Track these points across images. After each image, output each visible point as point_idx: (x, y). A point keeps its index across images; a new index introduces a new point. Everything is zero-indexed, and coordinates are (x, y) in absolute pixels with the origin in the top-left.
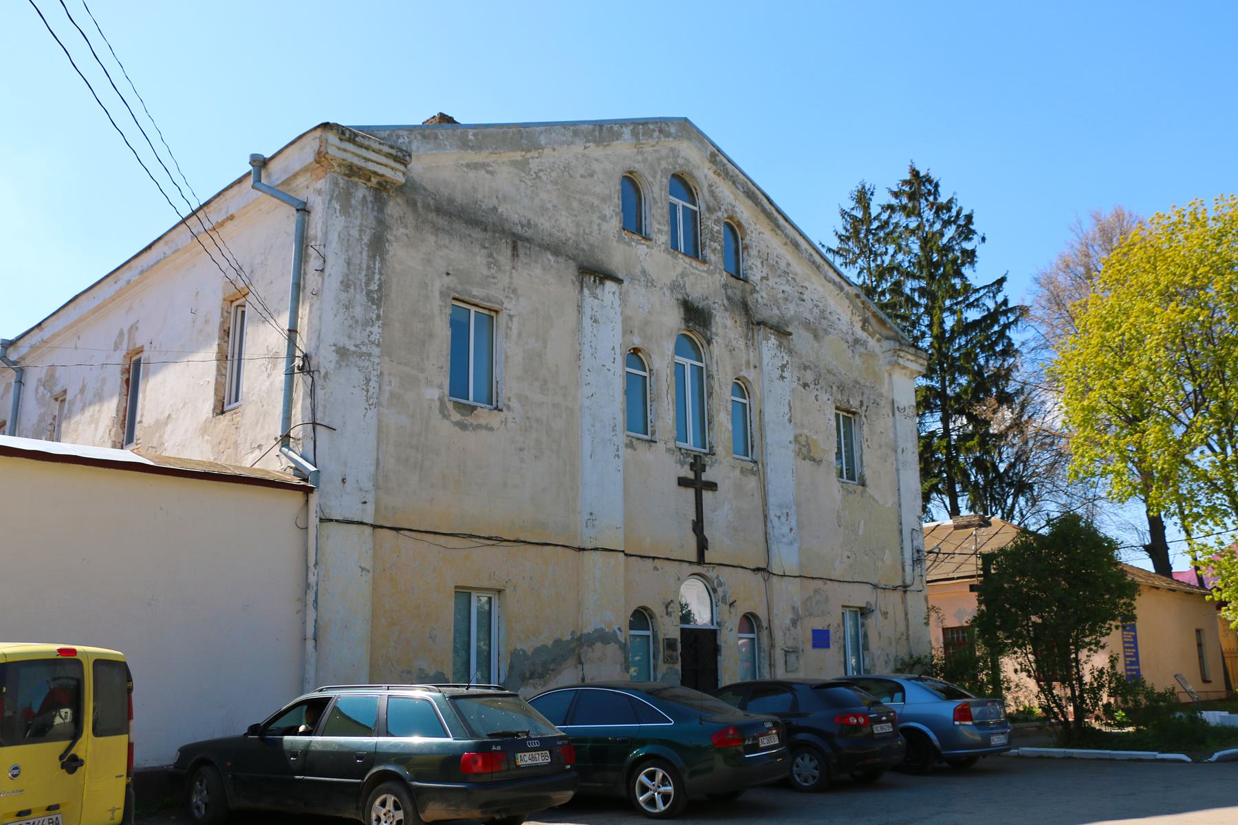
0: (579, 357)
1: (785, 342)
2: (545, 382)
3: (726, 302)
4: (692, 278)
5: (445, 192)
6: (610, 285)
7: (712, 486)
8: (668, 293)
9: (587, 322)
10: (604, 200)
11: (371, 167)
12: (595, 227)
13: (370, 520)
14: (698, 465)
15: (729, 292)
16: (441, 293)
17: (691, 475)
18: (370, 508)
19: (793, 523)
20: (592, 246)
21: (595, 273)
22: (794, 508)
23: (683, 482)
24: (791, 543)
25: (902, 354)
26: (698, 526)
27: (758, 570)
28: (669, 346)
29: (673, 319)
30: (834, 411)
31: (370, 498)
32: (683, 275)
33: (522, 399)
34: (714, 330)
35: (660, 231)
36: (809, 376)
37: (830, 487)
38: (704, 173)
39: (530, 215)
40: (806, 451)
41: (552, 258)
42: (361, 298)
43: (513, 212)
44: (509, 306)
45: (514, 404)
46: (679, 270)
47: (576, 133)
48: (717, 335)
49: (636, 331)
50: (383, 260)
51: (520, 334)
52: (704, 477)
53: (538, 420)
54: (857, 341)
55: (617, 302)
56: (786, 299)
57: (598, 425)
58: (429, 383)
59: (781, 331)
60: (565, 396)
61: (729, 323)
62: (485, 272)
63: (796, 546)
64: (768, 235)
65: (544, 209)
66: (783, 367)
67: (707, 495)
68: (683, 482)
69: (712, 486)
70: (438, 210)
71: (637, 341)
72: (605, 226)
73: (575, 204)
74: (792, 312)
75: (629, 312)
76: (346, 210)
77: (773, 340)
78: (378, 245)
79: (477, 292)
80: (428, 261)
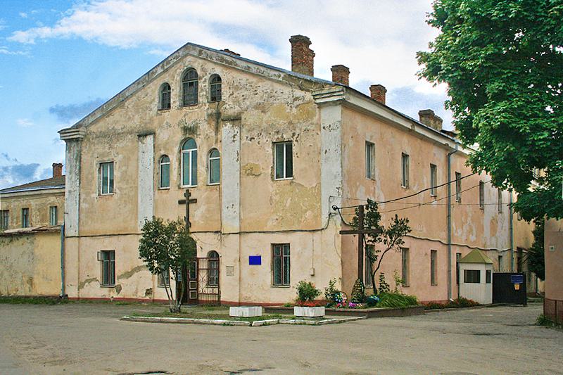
0: (138, 167)
1: (237, 122)
2: (128, 180)
3: (206, 118)
4: (190, 115)
5: (99, 130)
6: (148, 137)
7: (195, 201)
8: (177, 127)
9: (140, 154)
10: (151, 103)
11: (71, 137)
12: (148, 115)
13: (77, 235)
14: (188, 194)
15: (210, 111)
16: (96, 164)
17: (184, 198)
18: (77, 232)
19: (237, 208)
20: (146, 124)
21: (142, 135)
22: (238, 201)
23: (181, 202)
24: (234, 218)
25: (318, 97)
26: (187, 218)
27: (217, 232)
28: (176, 149)
29: (179, 136)
30: (271, 145)
31: (77, 229)
32: (185, 116)
33: (120, 189)
34: (198, 133)
35: (174, 102)
36: (255, 133)
37: (268, 186)
38: (197, 65)
39: (125, 123)
40: (249, 171)
41: (130, 136)
42: (74, 175)
43: (118, 127)
44: (116, 159)
45: (118, 191)
46: (183, 114)
47: (139, 84)
48: (200, 135)
49: (162, 149)
50: (80, 161)
51: (119, 167)
52: (190, 198)
53: (126, 194)
54: (296, 99)
55: (152, 139)
56: (244, 99)
57: (144, 190)
58: (93, 193)
59: (236, 119)
60: (134, 183)
61: (206, 126)
62: (108, 151)
63: (238, 219)
64: (235, 74)
65: (130, 118)
66: (234, 137)
67: (191, 206)
68: (181, 202)
69: (195, 201)
70: (96, 137)
71: (163, 152)
72: (151, 113)
73: (140, 110)
74: (248, 103)
75: (159, 143)
76: (69, 152)
77: (229, 125)
78: (79, 158)
79: (106, 159)
80: (92, 156)
